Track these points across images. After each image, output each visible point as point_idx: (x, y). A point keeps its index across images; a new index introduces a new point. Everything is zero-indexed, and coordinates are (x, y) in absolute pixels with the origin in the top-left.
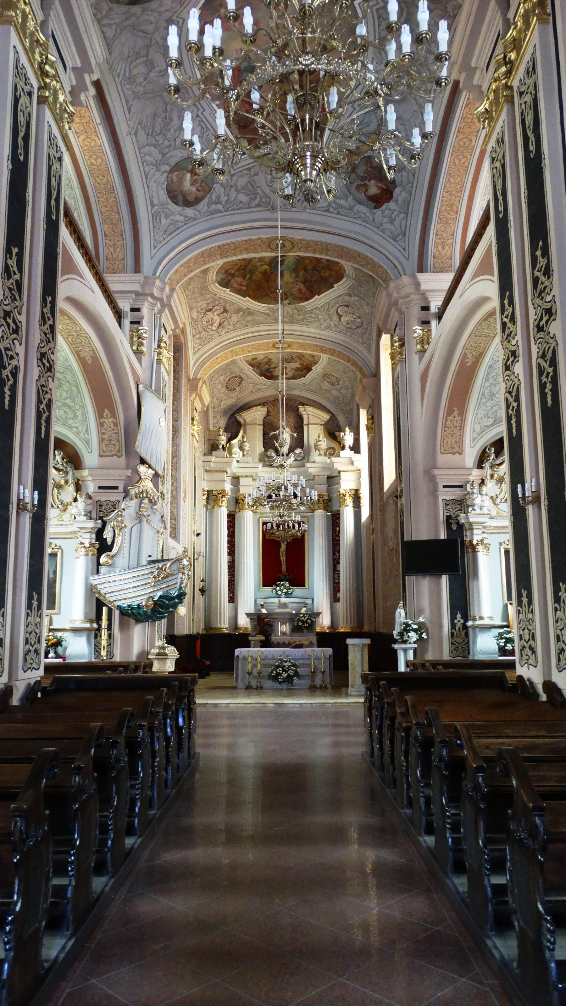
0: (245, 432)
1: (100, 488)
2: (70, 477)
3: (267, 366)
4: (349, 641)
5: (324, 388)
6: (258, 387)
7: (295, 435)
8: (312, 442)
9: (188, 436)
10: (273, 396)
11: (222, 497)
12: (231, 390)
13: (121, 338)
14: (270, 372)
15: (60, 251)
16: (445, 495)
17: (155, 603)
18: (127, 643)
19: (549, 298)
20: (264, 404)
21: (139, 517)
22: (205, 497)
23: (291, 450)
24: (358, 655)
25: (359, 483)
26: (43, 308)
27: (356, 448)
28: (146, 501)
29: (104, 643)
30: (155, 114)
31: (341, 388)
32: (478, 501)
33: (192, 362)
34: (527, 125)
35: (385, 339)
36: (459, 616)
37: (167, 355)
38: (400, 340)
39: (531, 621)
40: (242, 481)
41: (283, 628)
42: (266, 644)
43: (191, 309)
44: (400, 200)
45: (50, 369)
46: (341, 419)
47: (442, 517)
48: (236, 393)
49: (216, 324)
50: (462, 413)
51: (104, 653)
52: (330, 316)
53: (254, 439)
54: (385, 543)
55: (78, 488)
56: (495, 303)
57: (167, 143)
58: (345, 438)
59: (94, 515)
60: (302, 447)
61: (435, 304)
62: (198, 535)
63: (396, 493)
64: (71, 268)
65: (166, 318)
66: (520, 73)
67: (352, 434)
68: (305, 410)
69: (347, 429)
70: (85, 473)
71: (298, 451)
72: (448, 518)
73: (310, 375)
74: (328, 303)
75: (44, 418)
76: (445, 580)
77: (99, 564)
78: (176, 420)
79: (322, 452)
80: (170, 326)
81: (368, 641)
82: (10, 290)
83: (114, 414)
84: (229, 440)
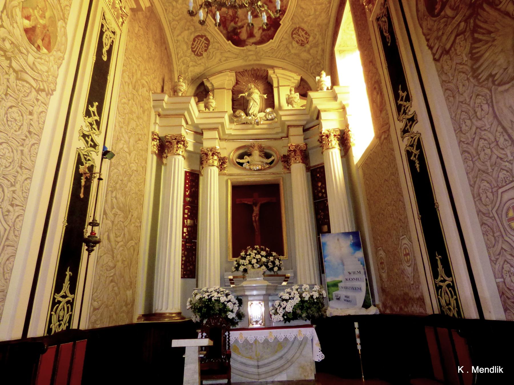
3: (232, 24)
5: (293, 51)
6: (226, 55)
7: (265, 96)
10: (241, 67)
11: (178, 142)
12: (197, 55)
14: (238, 34)
22: (155, 143)
31: (311, 47)
48: (203, 60)
53: (222, 102)
58: (322, 79)
67: (329, 77)
68: (274, 73)
69: (324, 73)
71: (269, 110)
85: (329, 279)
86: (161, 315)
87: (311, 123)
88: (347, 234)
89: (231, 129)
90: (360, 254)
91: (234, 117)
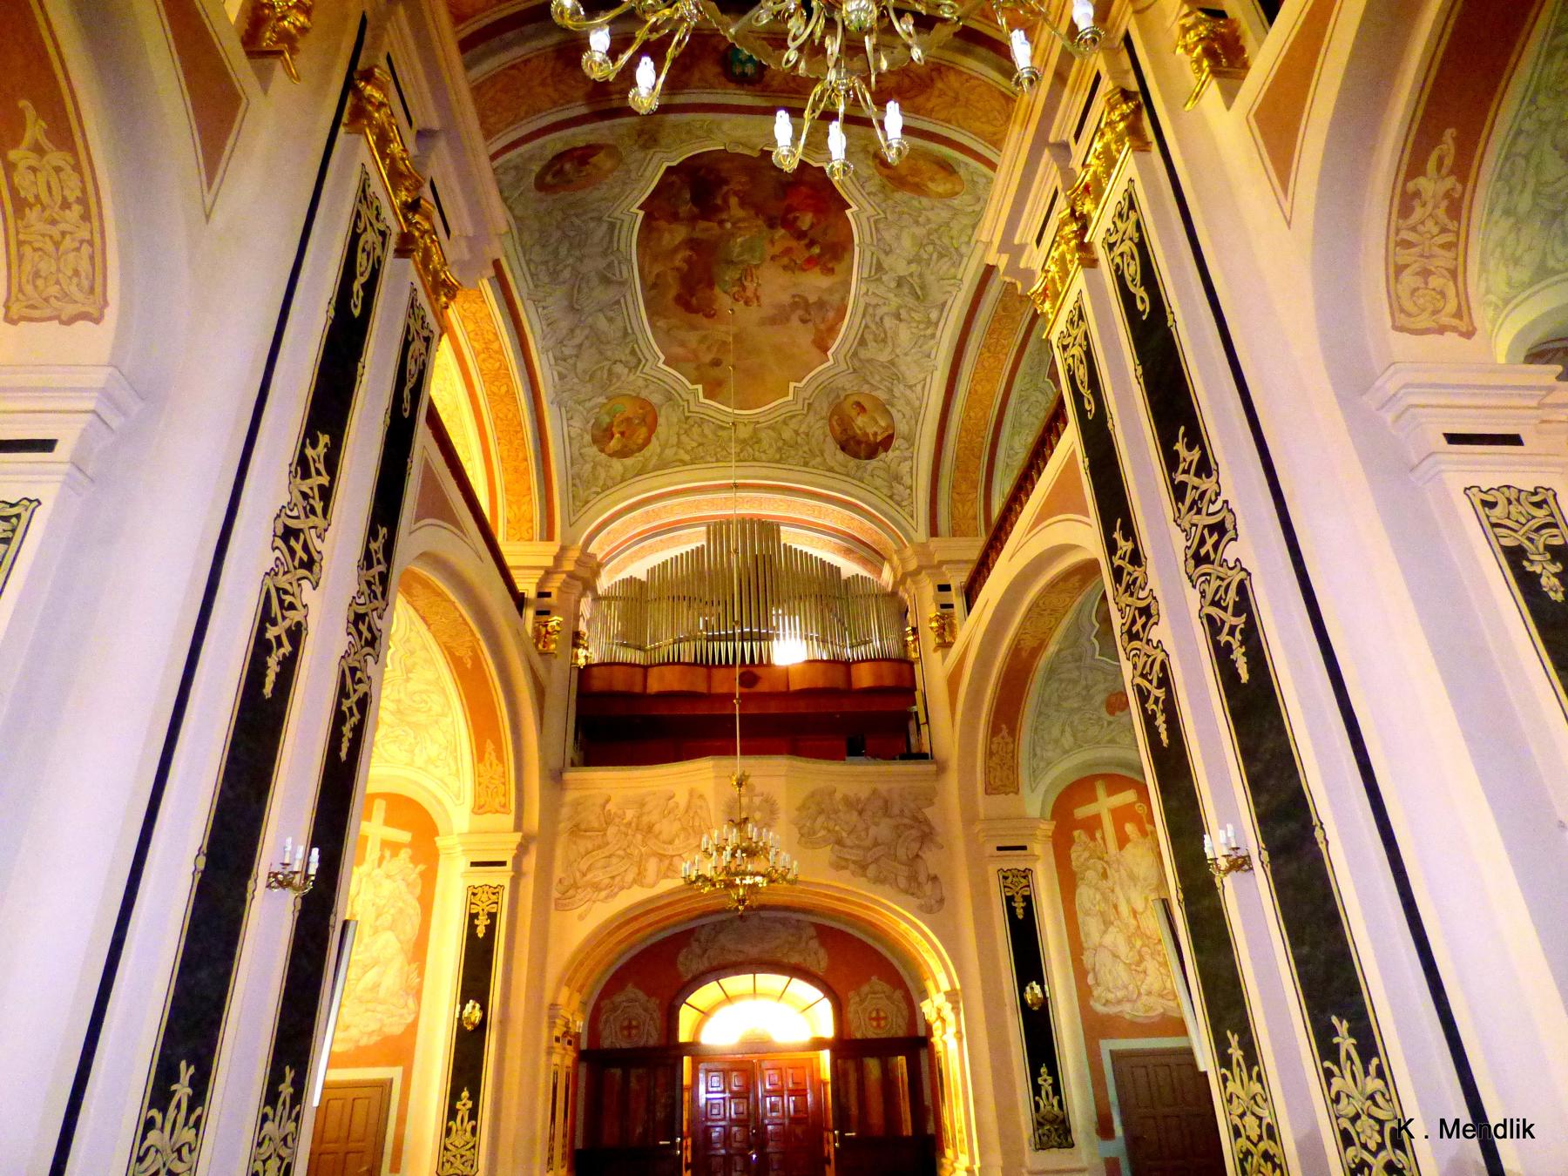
26: (368, 542)
34: (1128, 279)
45: (371, 643)
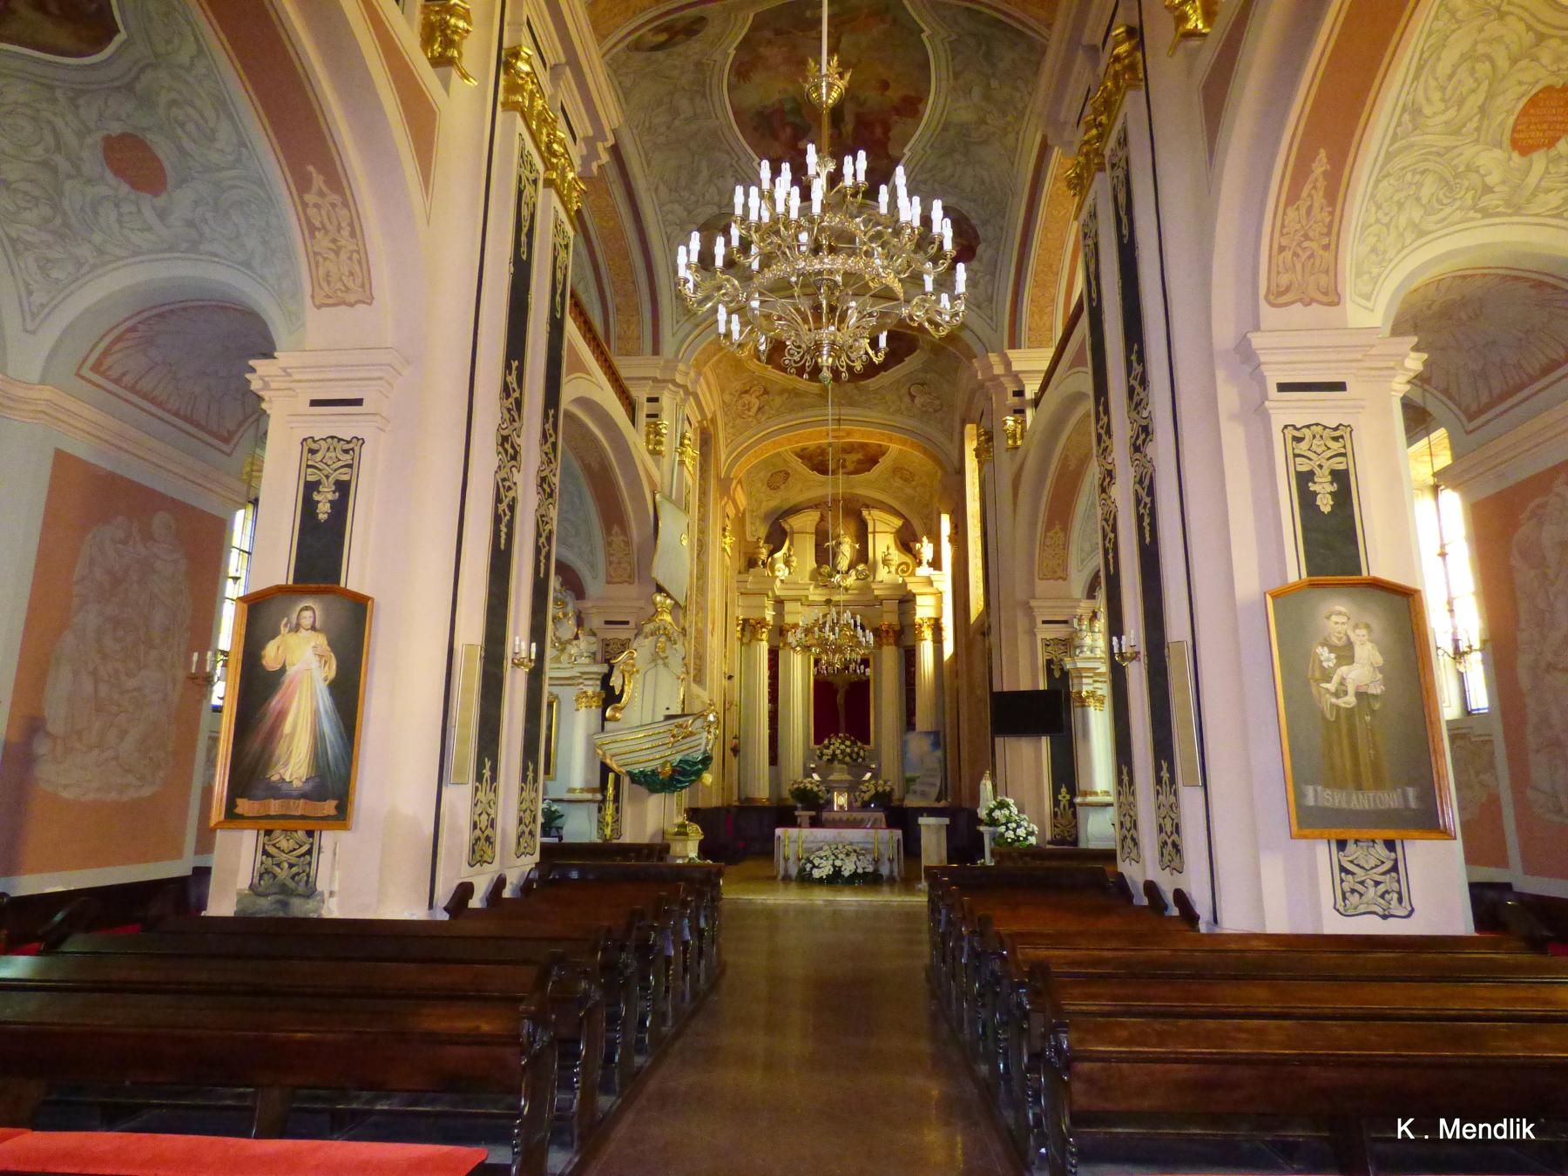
0: (791, 543)
1: (607, 622)
2: (570, 609)
4: (922, 821)
8: (879, 557)
9: (718, 553)
13: (637, 440)
15: (565, 353)
16: (1046, 633)
17: (674, 770)
18: (640, 819)
19: (1145, 414)
20: (816, 506)
21: (657, 658)
23: (852, 566)
24: (934, 838)
25: (940, 609)
27: (936, 564)
28: (663, 639)
29: (609, 819)
30: (680, 167)
32: (1088, 641)
33: (723, 458)
35: (970, 429)
36: (1064, 790)
37: (692, 452)
38: (986, 433)
39: (1132, 805)
40: (788, 606)
41: (840, 800)
42: (816, 823)
43: (723, 391)
44: (985, 260)
46: (917, 524)
47: (1041, 662)
49: (755, 409)
50: (1066, 528)
51: (608, 832)
52: (900, 398)
54: (971, 691)
55: (580, 622)
56: (1089, 404)
57: (693, 198)
59: (599, 657)
60: (866, 562)
61: (1031, 389)
62: (730, 677)
63: (984, 628)
64: (579, 366)
65: (690, 409)
66: (1112, 142)
69: (925, 539)
70: (587, 604)
71: (861, 567)
72: (1049, 662)
73: (876, 469)
74: (898, 381)
75: (544, 552)
76: (1045, 742)
77: (604, 719)
78: (703, 531)
79: (893, 569)
80: (695, 417)
81: (946, 821)
82: (509, 410)
83: (625, 529)
84: (771, 554)
85: (908, 775)
86: (753, 800)
87: (906, 601)
88: (928, 733)
89: (816, 595)
90: (939, 753)
91: (816, 575)
